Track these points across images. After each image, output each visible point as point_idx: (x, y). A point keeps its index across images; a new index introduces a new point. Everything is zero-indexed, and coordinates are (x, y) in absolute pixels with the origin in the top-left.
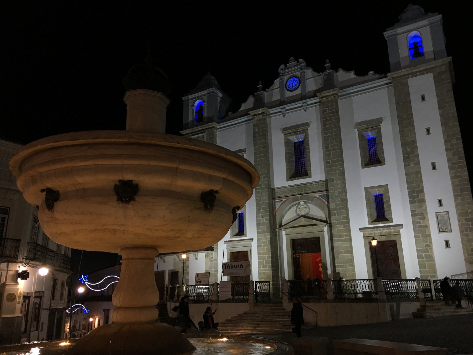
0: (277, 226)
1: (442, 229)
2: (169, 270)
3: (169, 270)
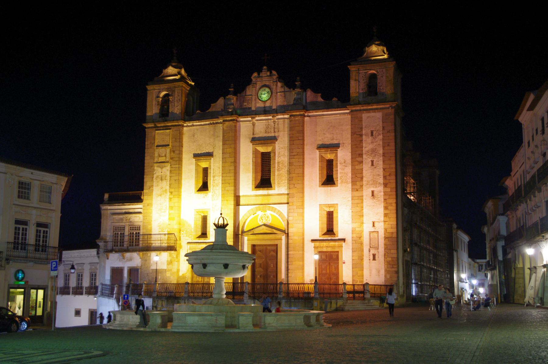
0: (240, 233)
1: (372, 245)
2: (128, 267)
3: (128, 267)
